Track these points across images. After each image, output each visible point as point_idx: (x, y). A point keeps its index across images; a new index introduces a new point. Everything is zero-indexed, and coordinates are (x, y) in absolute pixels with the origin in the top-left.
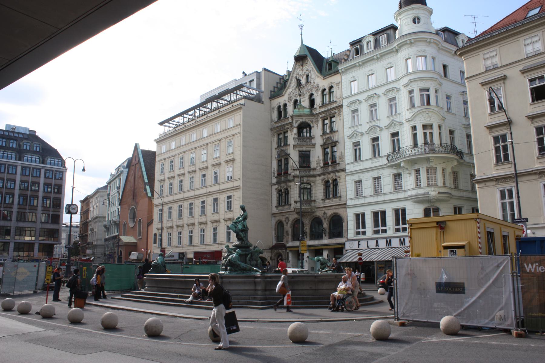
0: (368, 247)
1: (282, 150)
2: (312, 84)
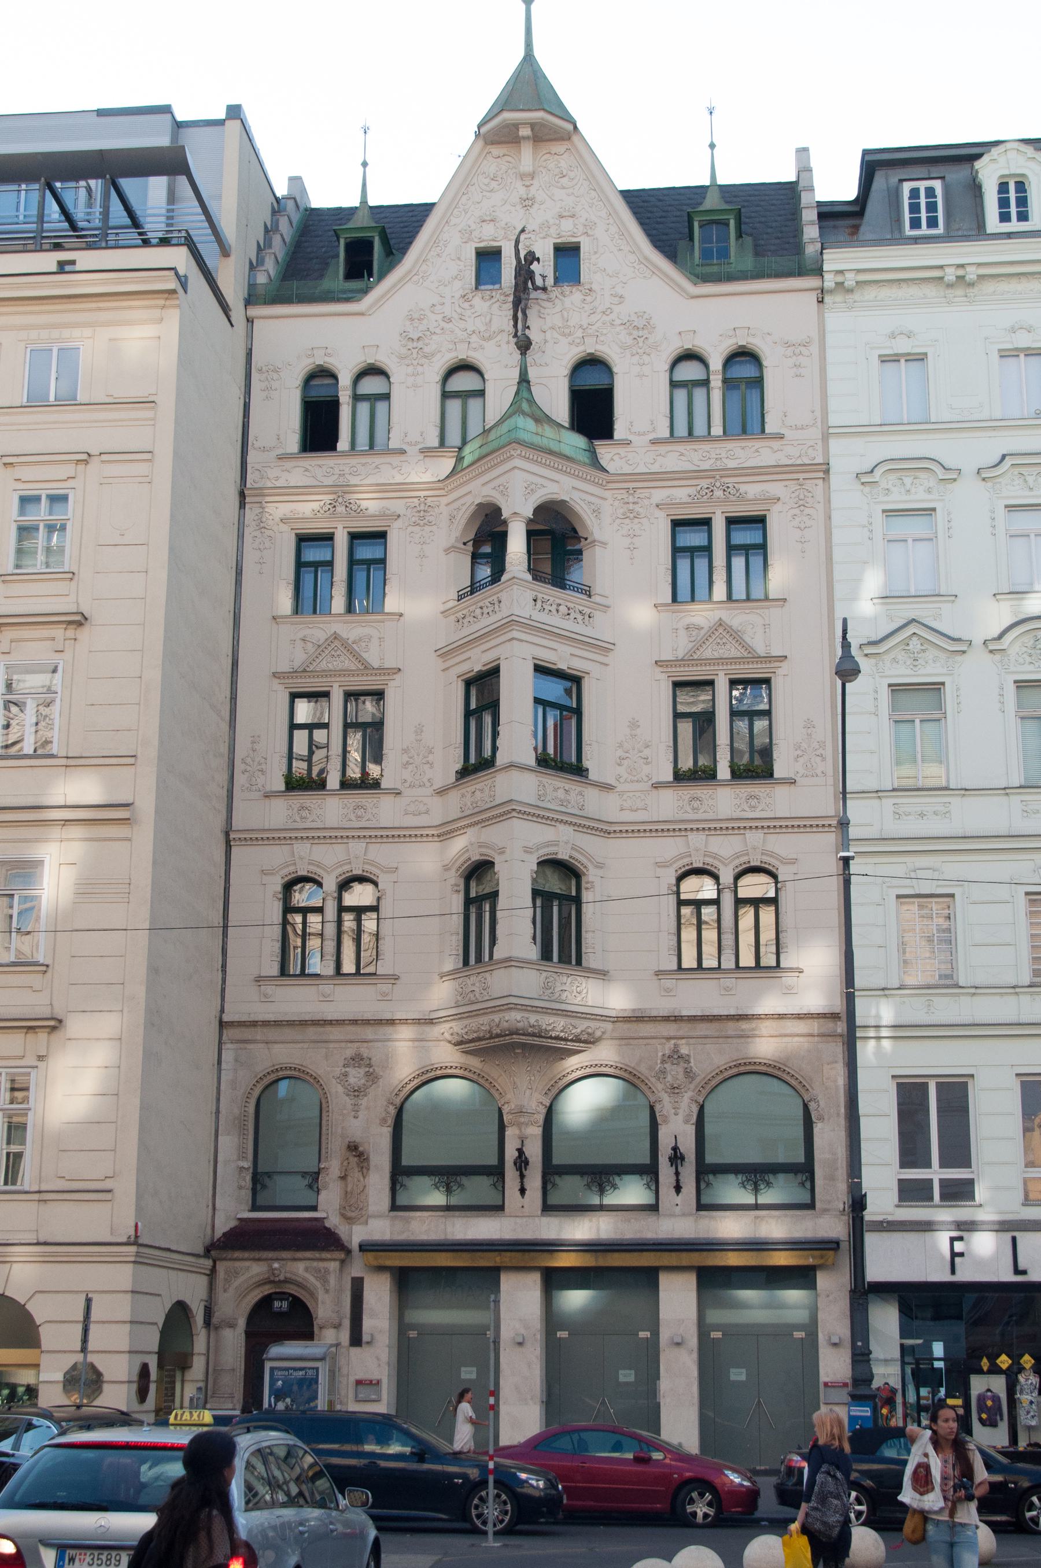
0: (1017, 1271)
1: (336, 636)
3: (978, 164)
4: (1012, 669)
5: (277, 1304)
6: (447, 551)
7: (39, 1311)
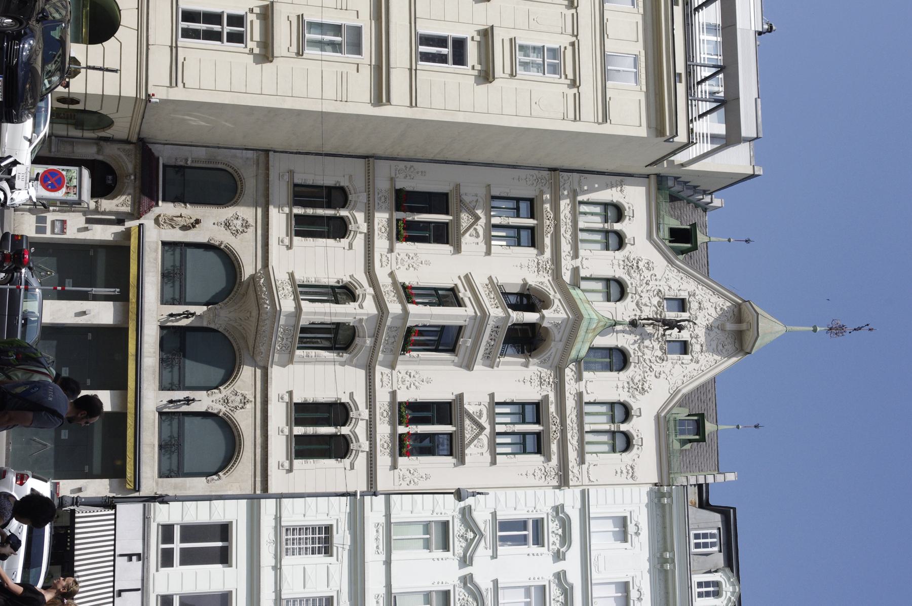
0: (120, 592)
2: (656, 367)
3: (727, 570)
4: (457, 589)
5: (110, 177)
6: (524, 280)
7: (110, 44)
